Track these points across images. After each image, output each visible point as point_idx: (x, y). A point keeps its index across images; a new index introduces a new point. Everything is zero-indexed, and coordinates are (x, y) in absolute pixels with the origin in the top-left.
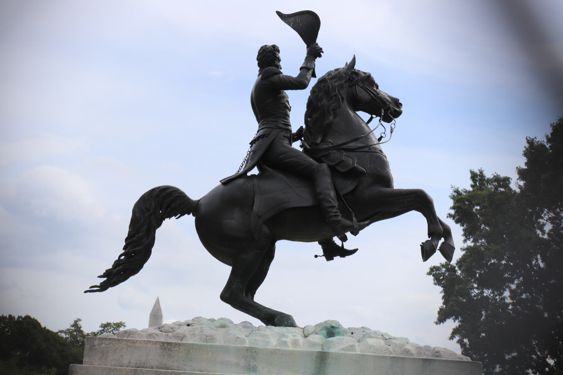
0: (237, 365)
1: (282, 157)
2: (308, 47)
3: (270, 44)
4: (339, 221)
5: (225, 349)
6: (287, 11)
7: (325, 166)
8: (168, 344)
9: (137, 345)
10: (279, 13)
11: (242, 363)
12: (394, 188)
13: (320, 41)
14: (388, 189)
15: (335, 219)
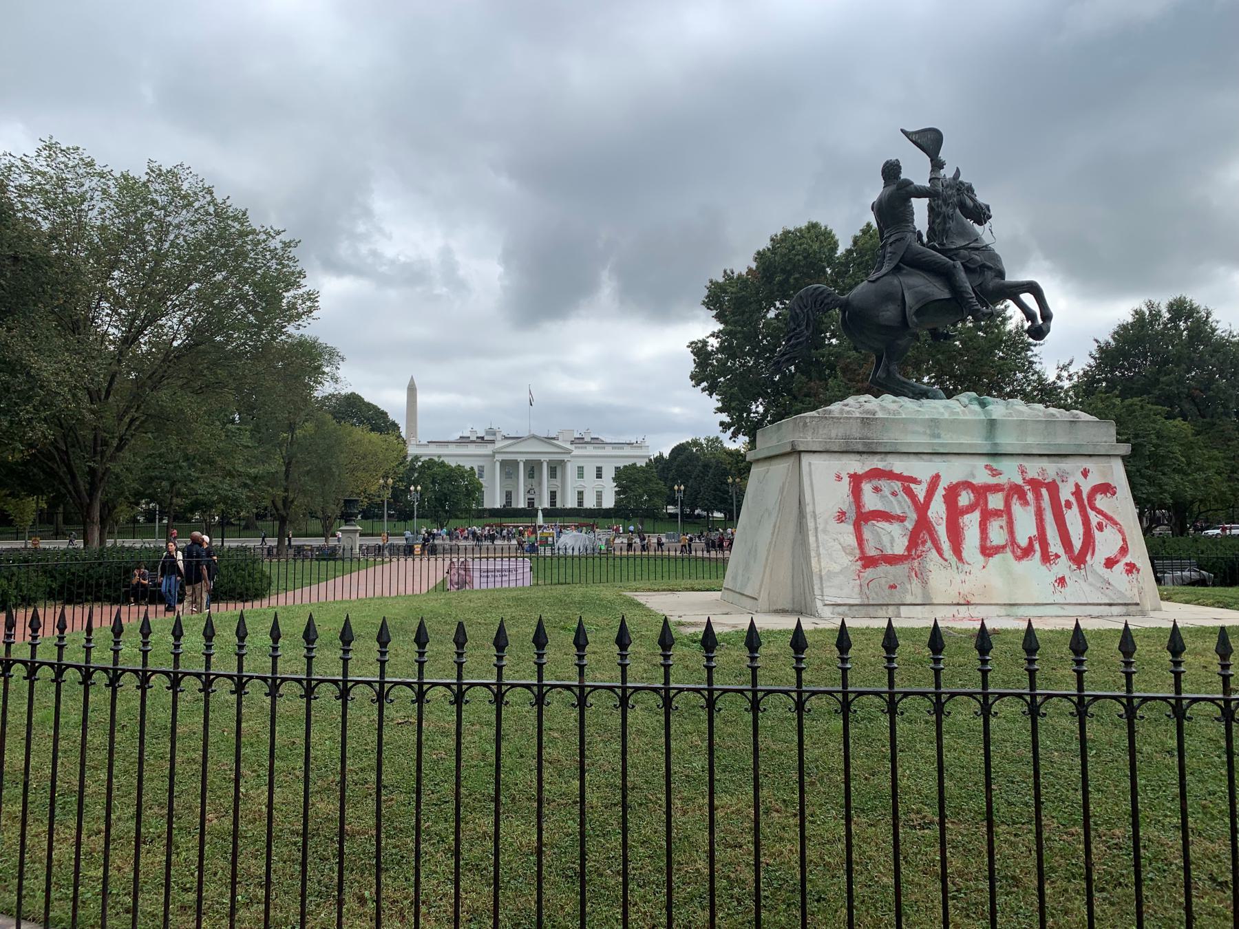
0: (925, 433)
1: (919, 256)
2: (931, 161)
3: (894, 159)
4: (978, 310)
5: (914, 421)
6: (910, 129)
7: (958, 264)
8: (867, 418)
9: (842, 421)
10: (902, 130)
11: (928, 432)
12: (1006, 279)
13: (942, 155)
14: (1003, 281)
15: (976, 307)
